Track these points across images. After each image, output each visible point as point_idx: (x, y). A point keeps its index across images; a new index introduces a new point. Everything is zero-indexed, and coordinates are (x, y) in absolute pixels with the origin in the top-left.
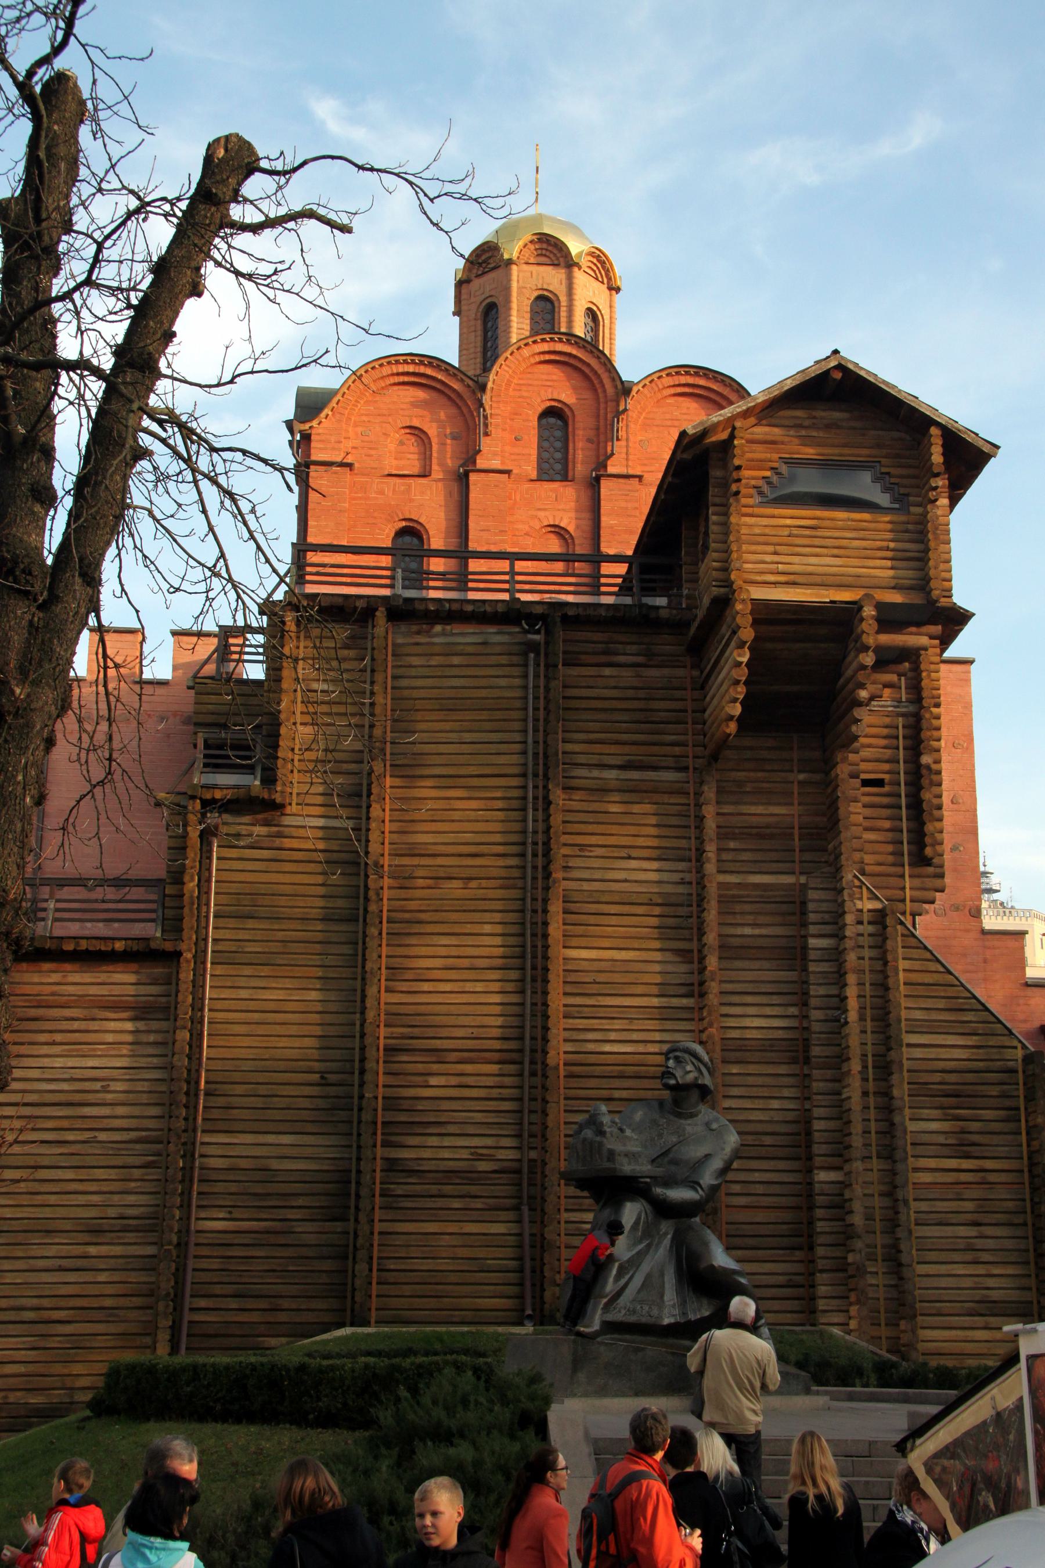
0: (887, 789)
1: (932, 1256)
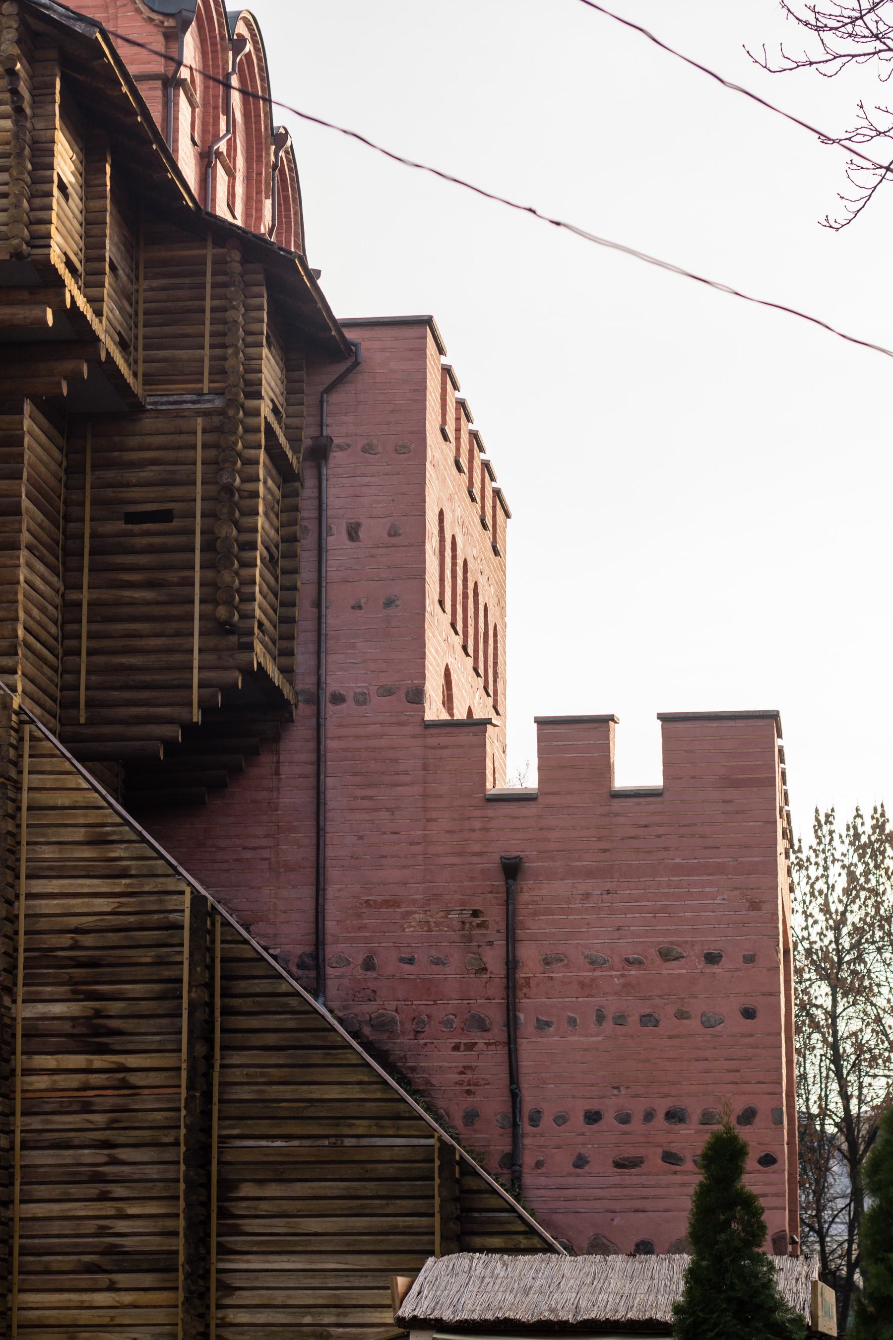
0: (176, 524)
1: (41, 1191)
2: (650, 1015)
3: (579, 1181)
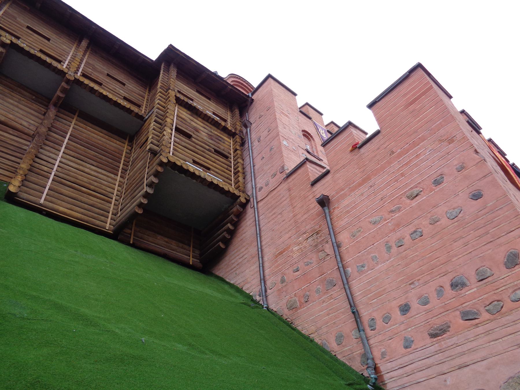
2: (415, 232)
3: (411, 357)
